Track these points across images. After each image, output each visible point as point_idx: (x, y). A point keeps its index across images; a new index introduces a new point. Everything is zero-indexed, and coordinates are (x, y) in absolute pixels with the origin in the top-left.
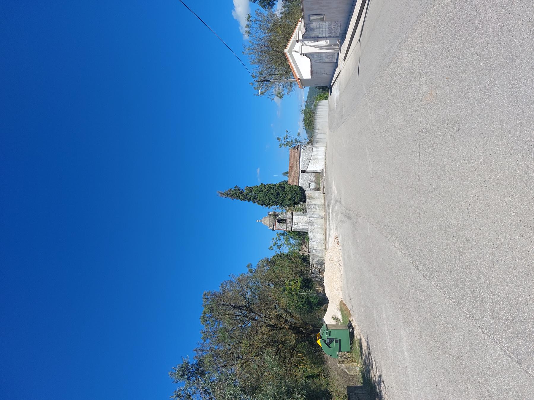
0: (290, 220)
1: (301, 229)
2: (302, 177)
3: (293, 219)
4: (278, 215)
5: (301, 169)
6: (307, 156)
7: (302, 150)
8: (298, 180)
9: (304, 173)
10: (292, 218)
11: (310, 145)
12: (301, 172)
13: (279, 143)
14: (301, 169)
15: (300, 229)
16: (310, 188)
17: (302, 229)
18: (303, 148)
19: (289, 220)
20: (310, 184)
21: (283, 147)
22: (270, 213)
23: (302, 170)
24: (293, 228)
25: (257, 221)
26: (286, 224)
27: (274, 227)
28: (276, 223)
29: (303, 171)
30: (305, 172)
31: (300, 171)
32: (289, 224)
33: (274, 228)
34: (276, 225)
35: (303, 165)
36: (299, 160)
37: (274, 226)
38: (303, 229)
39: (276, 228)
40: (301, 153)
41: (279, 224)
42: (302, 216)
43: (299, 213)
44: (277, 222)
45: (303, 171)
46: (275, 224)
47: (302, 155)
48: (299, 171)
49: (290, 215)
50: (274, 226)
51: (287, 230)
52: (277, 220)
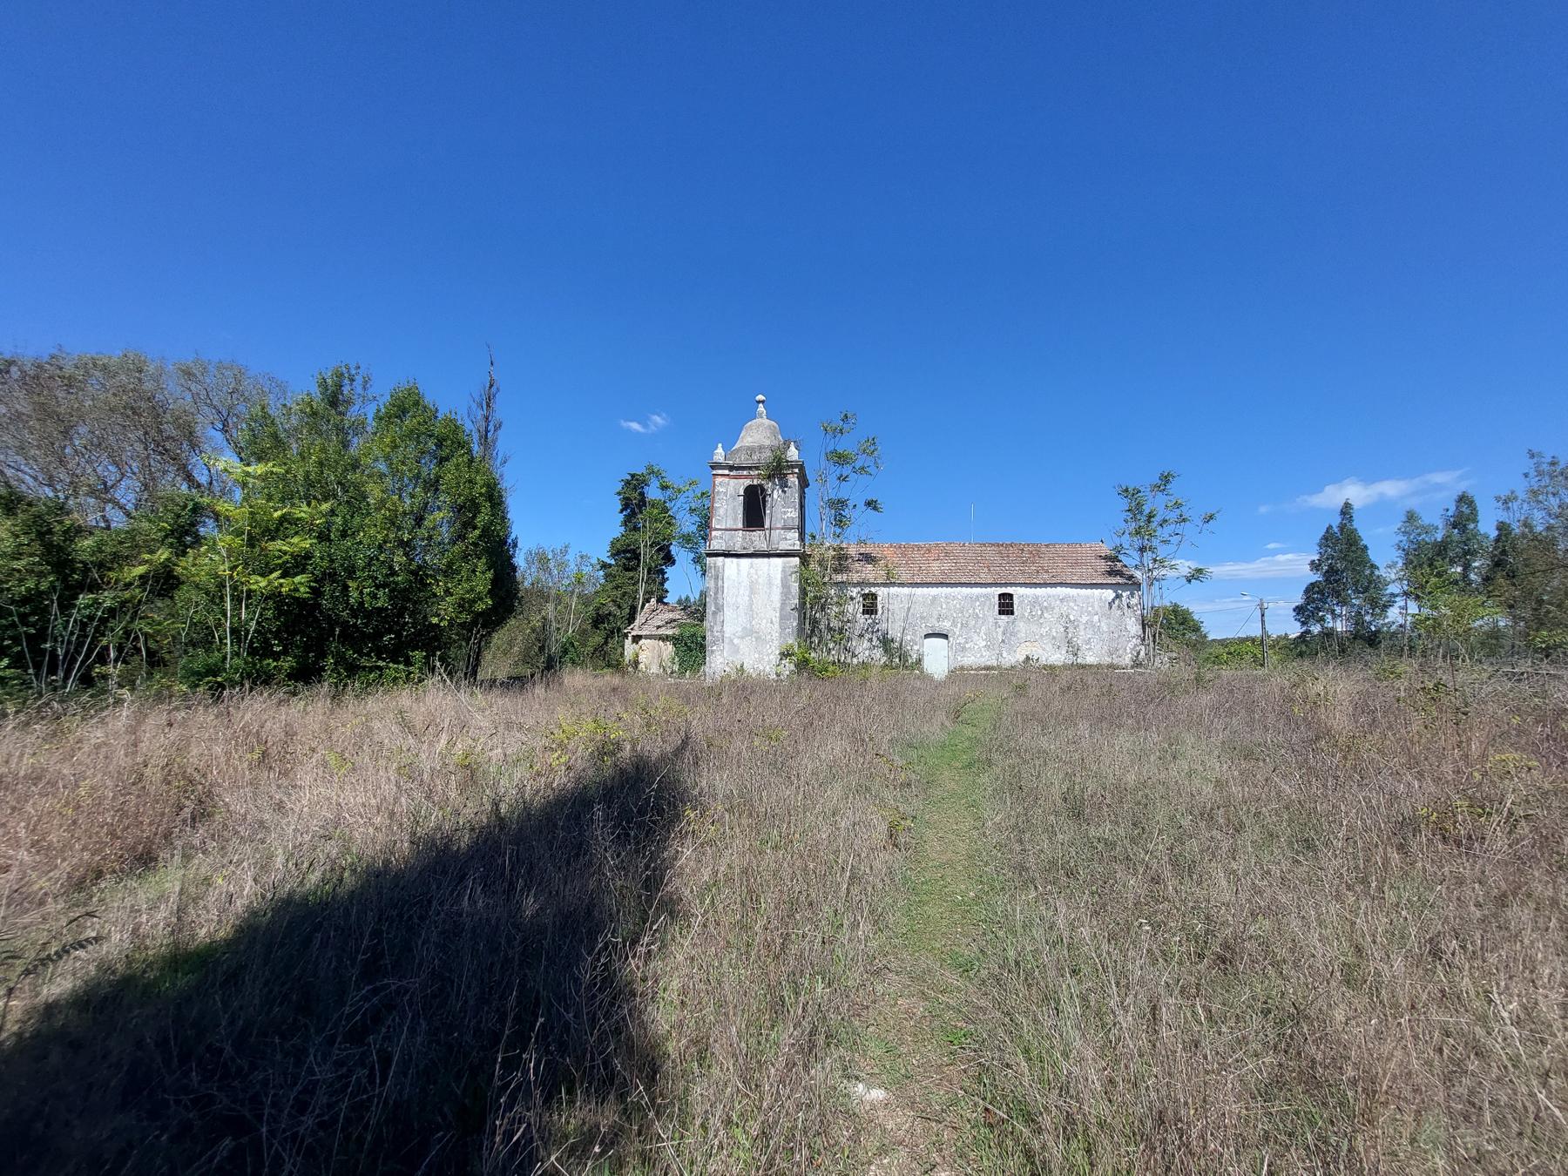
0: (763, 546)
1: (716, 599)
2: (978, 598)
3: (766, 560)
4: (781, 487)
6: (1084, 619)
7: (1109, 594)
8: (963, 580)
9: (997, 607)
11: (1140, 632)
12: (1002, 596)
13: (1143, 479)
16: (927, 636)
17: (716, 604)
18: (1118, 596)
19: (757, 540)
20: (945, 637)
21: (1124, 504)
22: (792, 448)
23: (1011, 596)
24: (721, 559)
25: (760, 397)
26: (740, 525)
27: (727, 472)
28: (746, 477)
29: (1006, 605)
30: (1001, 613)
31: (1009, 590)
32: (739, 541)
33: (720, 472)
34: (735, 477)
35: (1035, 602)
36: (1061, 584)
37: (731, 468)
38: (719, 609)
39: (719, 480)
40: (1097, 592)
42: (783, 604)
43: (795, 587)
44: (748, 482)
45: (1006, 605)
46: (740, 472)
48: (1006, 585)
49: (784, 546)
50: (731, 468)
51: (714, 533)
52: (755, 482)
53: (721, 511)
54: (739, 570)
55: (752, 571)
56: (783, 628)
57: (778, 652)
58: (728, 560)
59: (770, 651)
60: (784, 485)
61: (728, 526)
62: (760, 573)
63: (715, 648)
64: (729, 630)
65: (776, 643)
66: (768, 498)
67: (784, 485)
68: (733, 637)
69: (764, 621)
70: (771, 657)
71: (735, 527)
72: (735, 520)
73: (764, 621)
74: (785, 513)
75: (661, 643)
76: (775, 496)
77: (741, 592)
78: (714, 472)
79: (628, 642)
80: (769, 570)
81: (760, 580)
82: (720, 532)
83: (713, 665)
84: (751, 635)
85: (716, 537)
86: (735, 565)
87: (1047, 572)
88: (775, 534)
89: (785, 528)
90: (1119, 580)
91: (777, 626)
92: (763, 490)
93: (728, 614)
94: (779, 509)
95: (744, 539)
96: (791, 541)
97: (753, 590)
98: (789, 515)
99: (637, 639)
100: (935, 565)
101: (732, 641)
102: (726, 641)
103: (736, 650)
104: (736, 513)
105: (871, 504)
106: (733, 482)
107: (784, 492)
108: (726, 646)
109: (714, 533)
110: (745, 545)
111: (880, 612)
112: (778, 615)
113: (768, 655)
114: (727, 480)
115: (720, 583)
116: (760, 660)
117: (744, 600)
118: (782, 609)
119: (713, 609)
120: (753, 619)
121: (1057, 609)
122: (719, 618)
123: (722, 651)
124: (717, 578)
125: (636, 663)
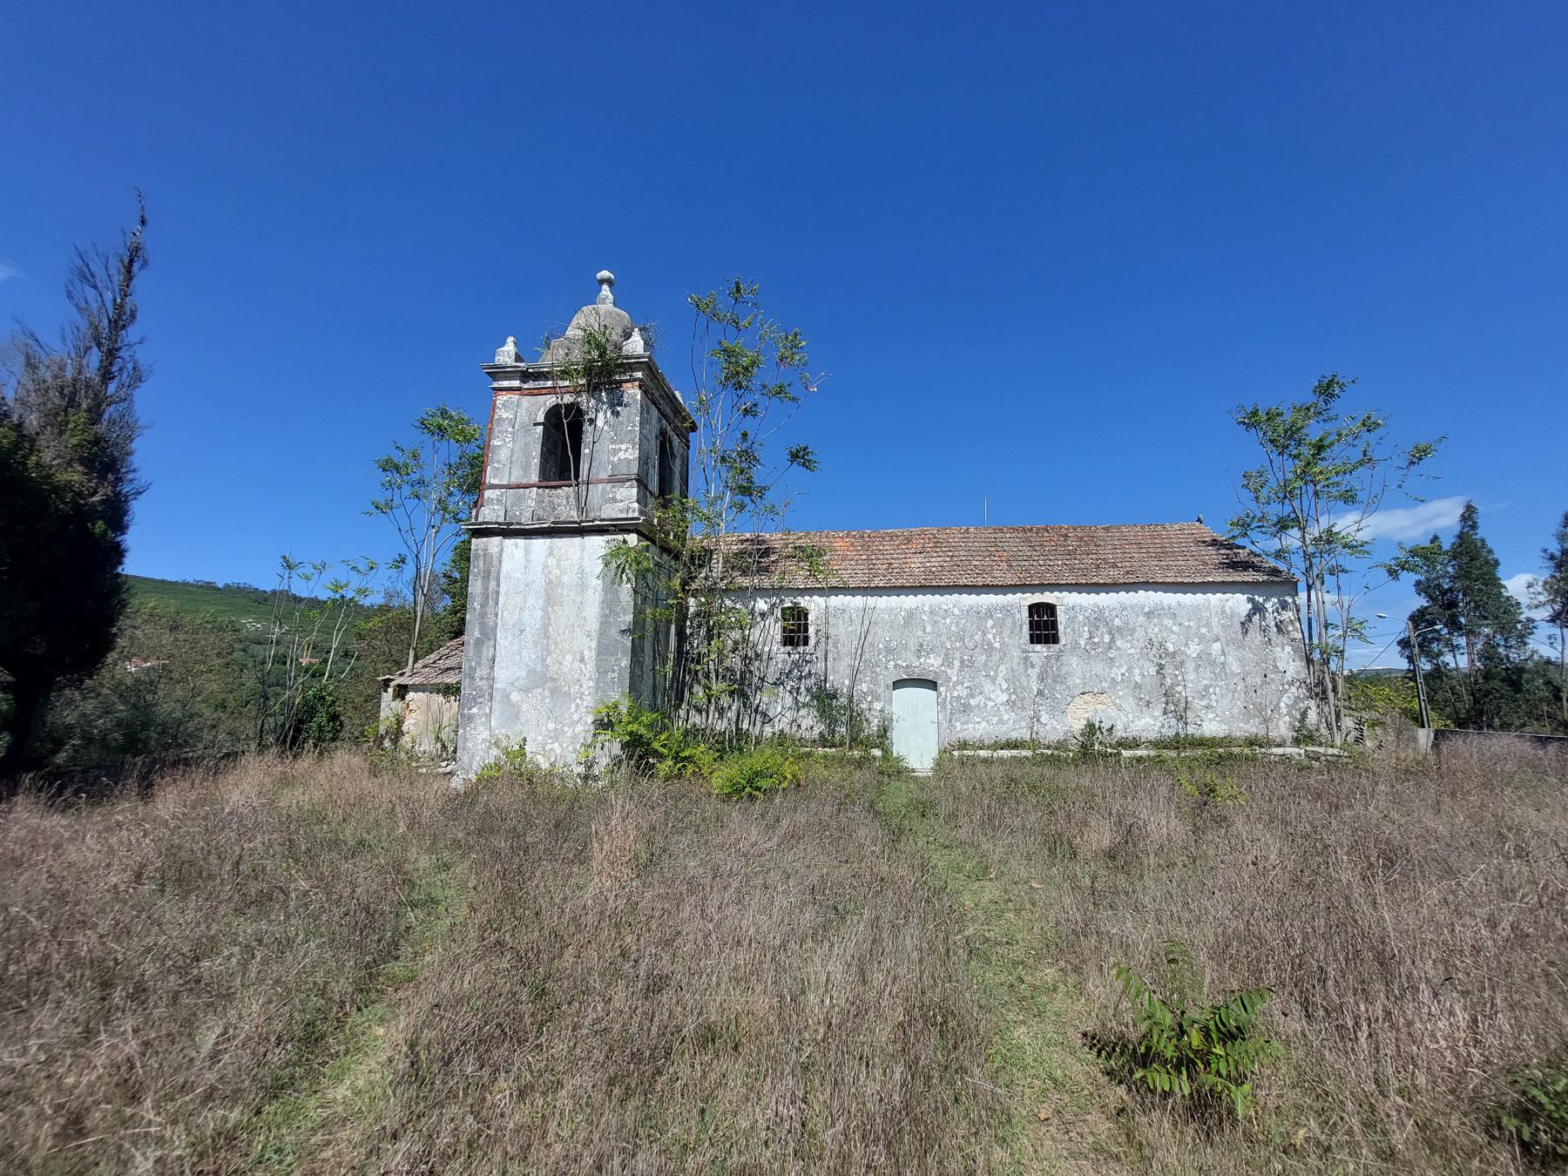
0: (569, 513)
1: (483, 615)
2: (990, 613)
3: (577, 540)
4: (612, 405)
5: (1063, 601)
6: (1194, 650)
7: (1239, 603)
8: (962, 582)
9: (1026, 628)
10: (580, 531)
12: (1034, 609)
14: (1063, 601)
15: (484, 605)
16: (898, 684)
17: (483, 625)
18: (1257, 609)
19: (563, 503)
20: (932, 685)
23: (1050, 609)
24: (496, 540)
25: (605, 274)
27: (516, 383)
28: (553, 391)
29: (1043, 626)
30: (1034, 639)
32: (530, 506)
33: (506, 384)
34: (533, 393)
35: (1098, 619)
37: (525, 376)
39: (502, 398)
40: (1215, 599)
41: (541, 418)
42: (605, 624)
44: (551, 400)
45: (1043, 626)
46: (541, 384)
47: (1197, 609)
48: (1042, 587)
49: (611, 512)
50: (525, 376)
52: (568, 399)
53: (503, 454)
54: (527, 561)
55: (552, 562)
56: (602, 670)
57: (590, 719)
58: (509, 542)
59: (576, 717)
60: (616, 403)
61: (514, 481)
62: (565, 564)
63: (474, 710)
64: (503, 675)
65: (589, 701)
66: (587, 427)
67: (616, 403)
68: (510, 688)
69: (569, 658)
70: (579, 728)
71: (525, 481)
72: (526, 468)
73: (569, 658)
74: (615, 452)
75: (440, 698)
76: (600, 423)
77: (530, 602)
78: (495, 385)
79: (387, 696)
80: (581, 558)
81: (565, 579)
82: (498, 492)
83: (469, 745)
84: (541, 685)
85: (491, 500)
86: (519, 553)
87: (1114, 566)
88: (596, 491)
89: (615, 480)
90: (1249, 576)
91: (590, 667)
92: (580, 413)
93: (504, 641)
94: (605, 446)
95: (540, 502)
96: (624, 502)
97: (551, 598)
98: (622, 455)
99: (402, 691)
100: (916, 562)
101: (507, 697)
102: (497, 696)
103: (514, 714)
104: (528, 458)
105: (799, 456)
106: (526, 401)
107: (617, 414)
108: (496, 706)
109: (488, 494)
110: (541, 513)
111: (812, 641)
112: (594, 644)
113: (574, 724)
114: (515, 397)
115: (492, 585)
116: (557, 735)
117: (533, 619)
118: (602, 633)
119: (477, 634)
120: (549, 653)
121: (1140, 633)
122: (487, 653)
123: (489, 716)
124: (487, 576)
125: (397, 733)
